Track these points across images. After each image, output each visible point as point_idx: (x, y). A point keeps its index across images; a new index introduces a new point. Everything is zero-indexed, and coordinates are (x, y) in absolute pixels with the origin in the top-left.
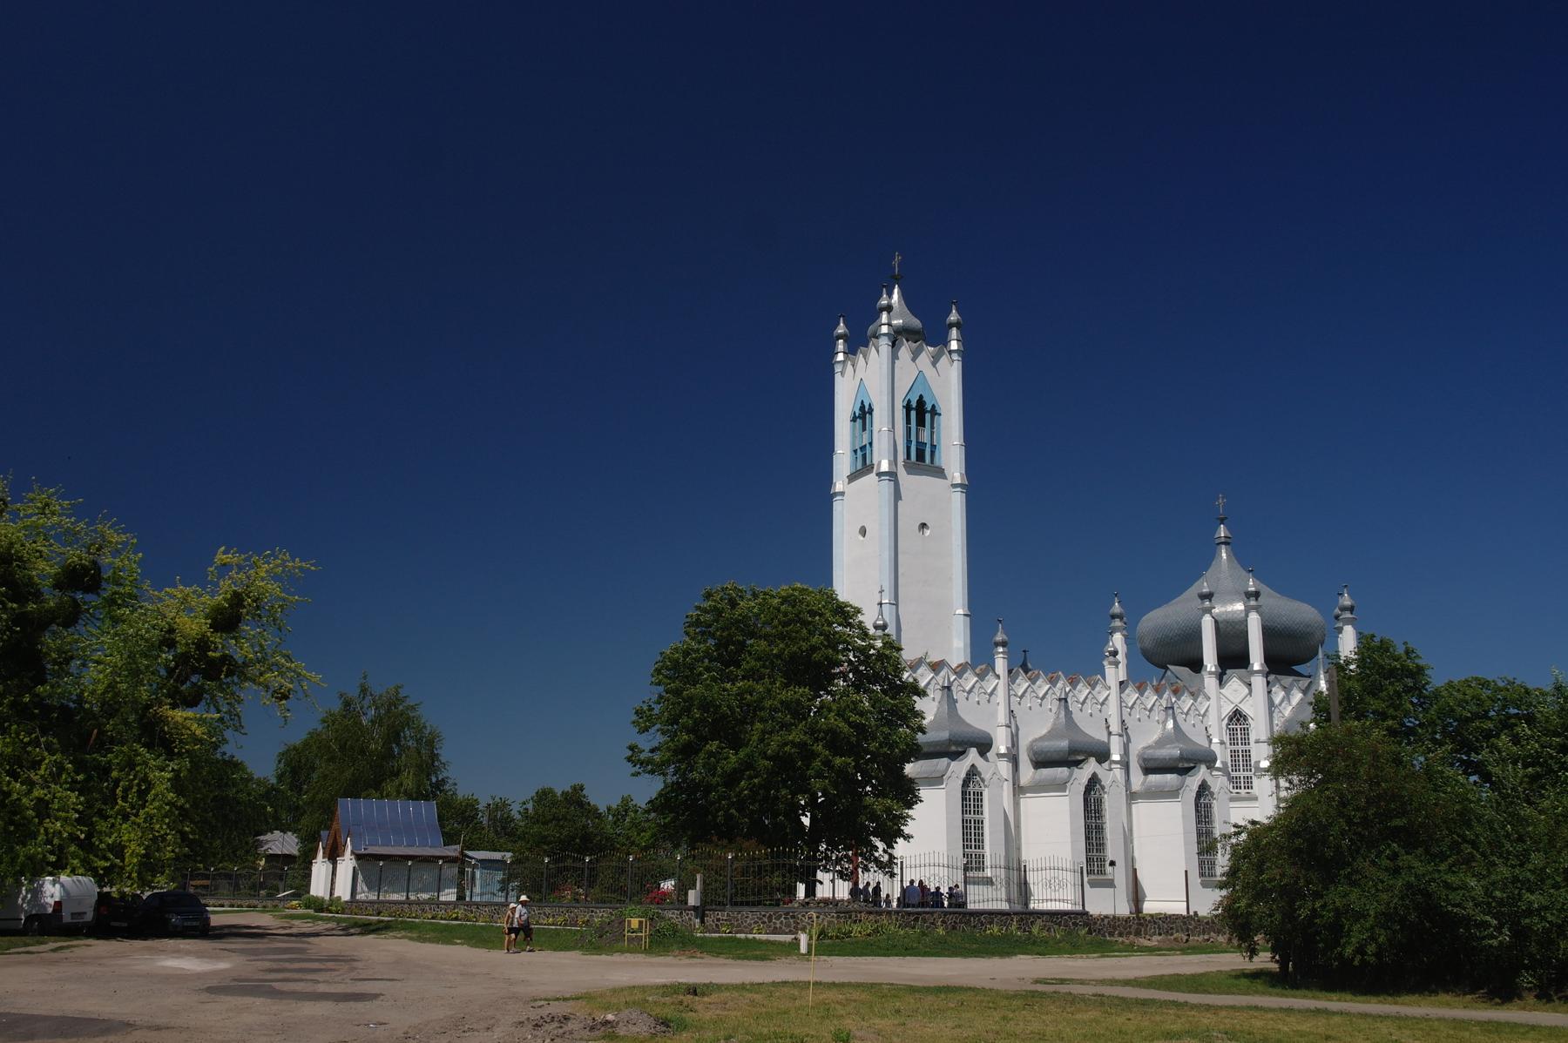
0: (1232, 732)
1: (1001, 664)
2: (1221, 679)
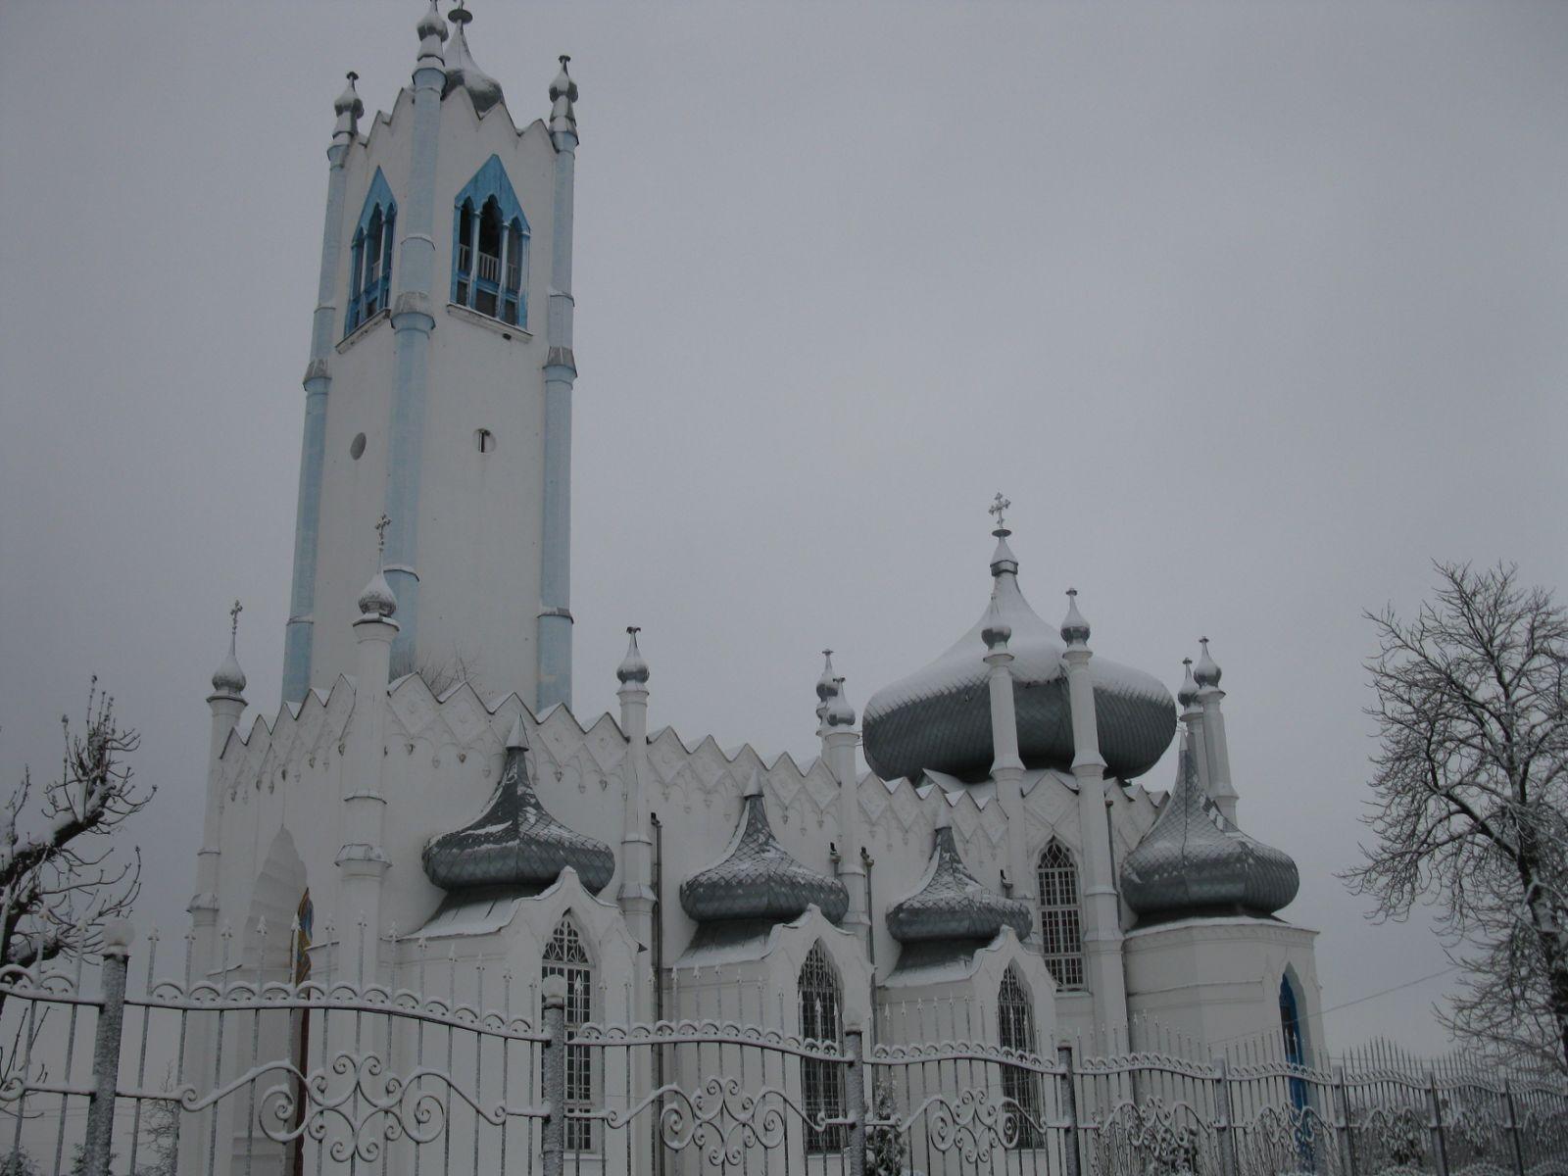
0: (1045, 880)
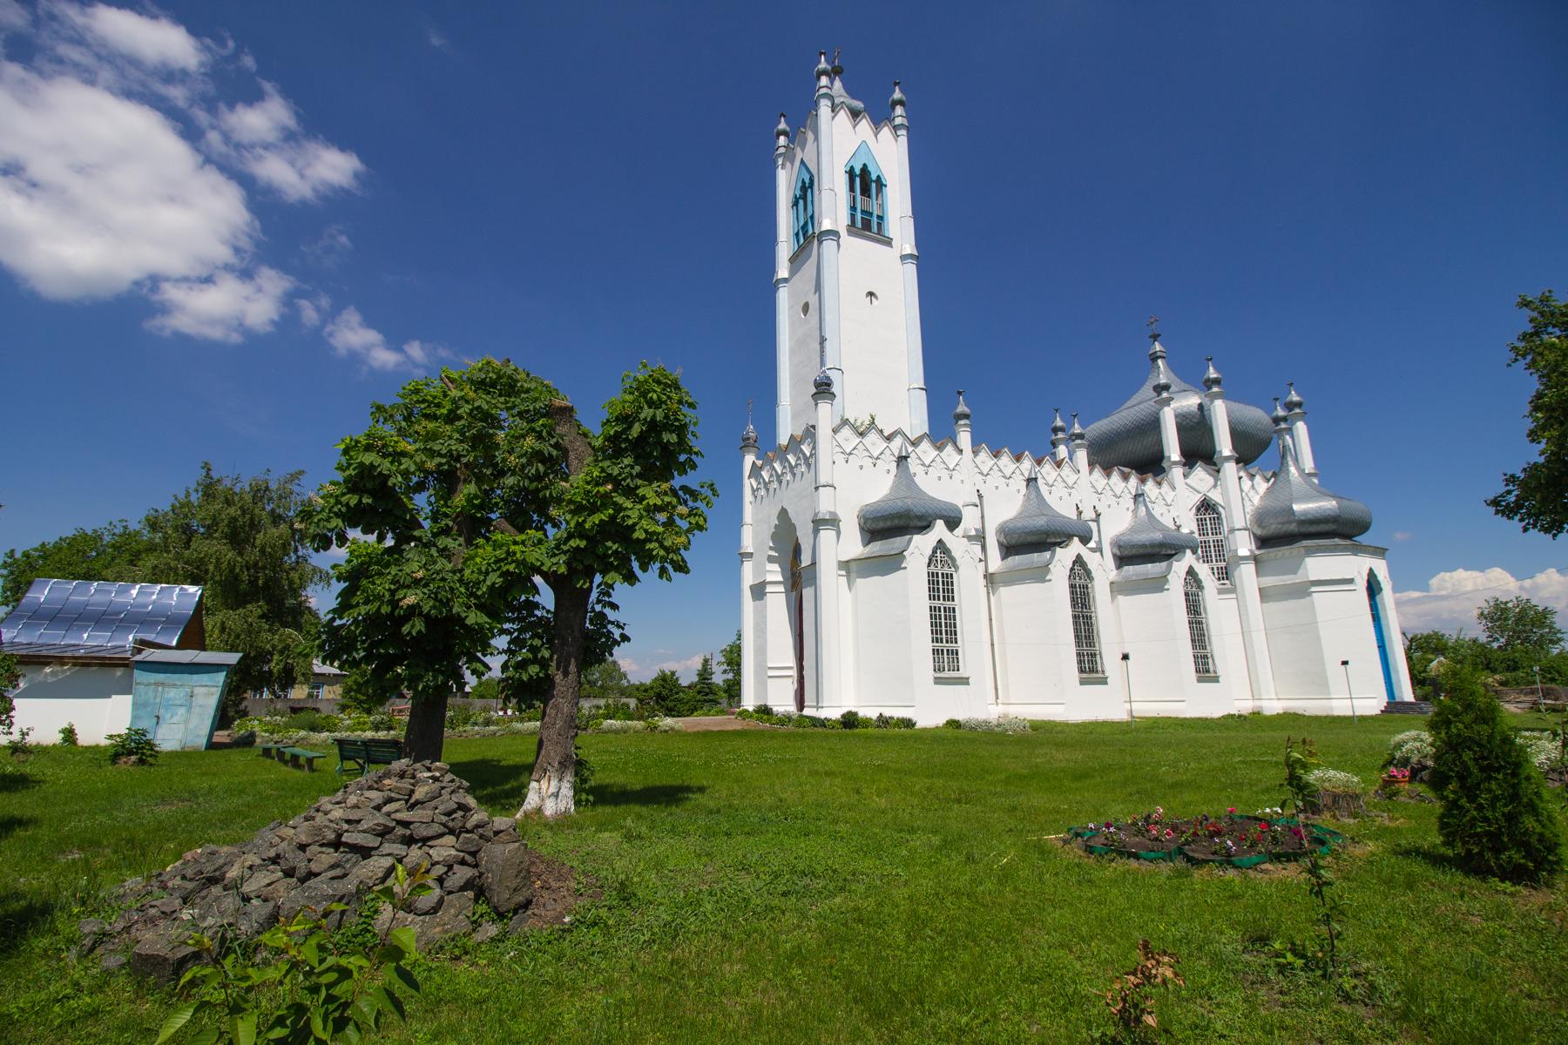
0: (1201, 523)
1: (965, 438)
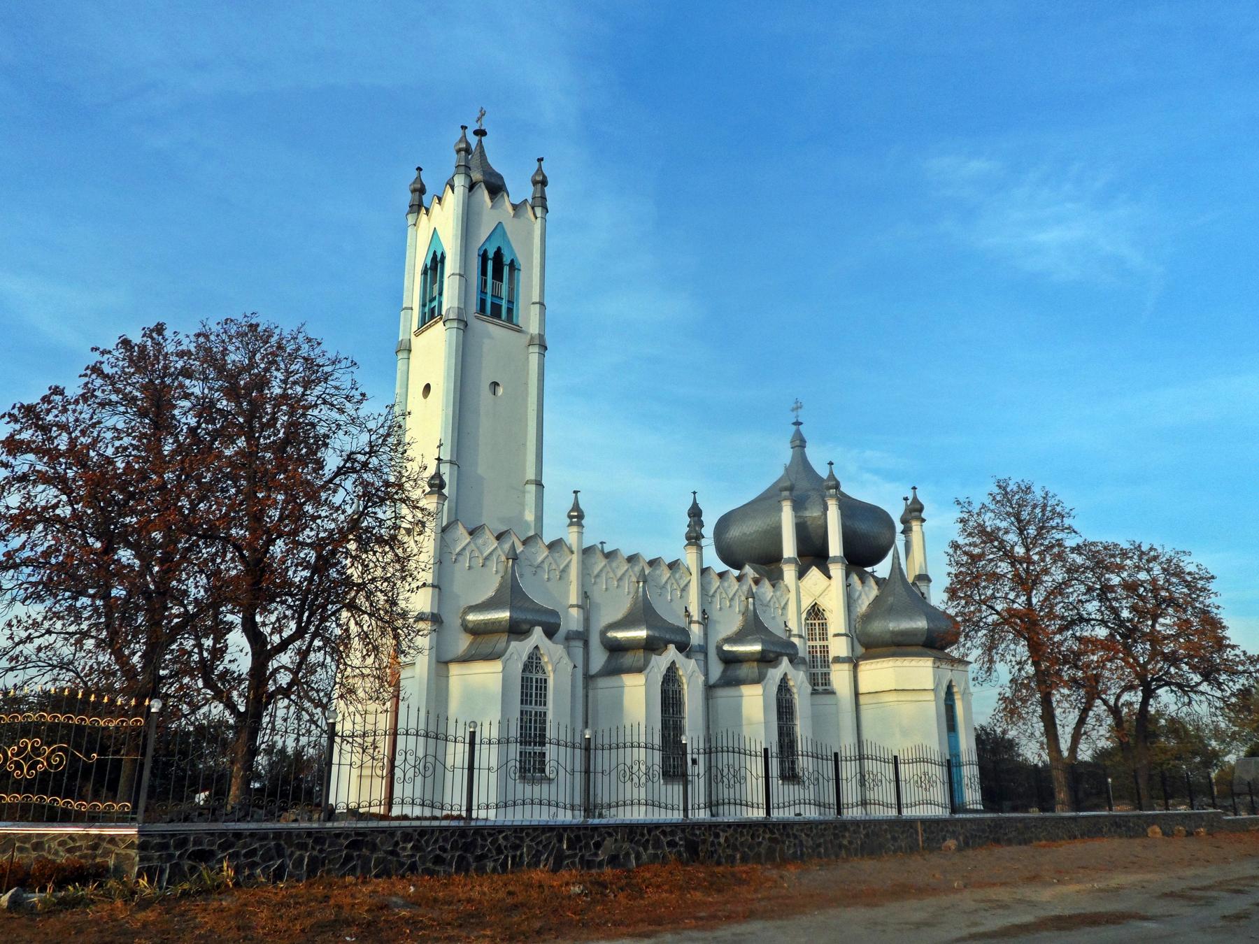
2: (801, 574)
